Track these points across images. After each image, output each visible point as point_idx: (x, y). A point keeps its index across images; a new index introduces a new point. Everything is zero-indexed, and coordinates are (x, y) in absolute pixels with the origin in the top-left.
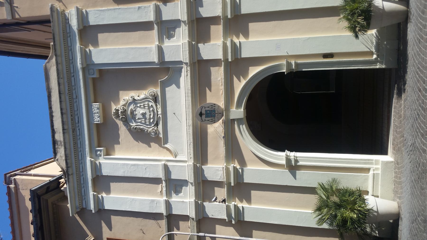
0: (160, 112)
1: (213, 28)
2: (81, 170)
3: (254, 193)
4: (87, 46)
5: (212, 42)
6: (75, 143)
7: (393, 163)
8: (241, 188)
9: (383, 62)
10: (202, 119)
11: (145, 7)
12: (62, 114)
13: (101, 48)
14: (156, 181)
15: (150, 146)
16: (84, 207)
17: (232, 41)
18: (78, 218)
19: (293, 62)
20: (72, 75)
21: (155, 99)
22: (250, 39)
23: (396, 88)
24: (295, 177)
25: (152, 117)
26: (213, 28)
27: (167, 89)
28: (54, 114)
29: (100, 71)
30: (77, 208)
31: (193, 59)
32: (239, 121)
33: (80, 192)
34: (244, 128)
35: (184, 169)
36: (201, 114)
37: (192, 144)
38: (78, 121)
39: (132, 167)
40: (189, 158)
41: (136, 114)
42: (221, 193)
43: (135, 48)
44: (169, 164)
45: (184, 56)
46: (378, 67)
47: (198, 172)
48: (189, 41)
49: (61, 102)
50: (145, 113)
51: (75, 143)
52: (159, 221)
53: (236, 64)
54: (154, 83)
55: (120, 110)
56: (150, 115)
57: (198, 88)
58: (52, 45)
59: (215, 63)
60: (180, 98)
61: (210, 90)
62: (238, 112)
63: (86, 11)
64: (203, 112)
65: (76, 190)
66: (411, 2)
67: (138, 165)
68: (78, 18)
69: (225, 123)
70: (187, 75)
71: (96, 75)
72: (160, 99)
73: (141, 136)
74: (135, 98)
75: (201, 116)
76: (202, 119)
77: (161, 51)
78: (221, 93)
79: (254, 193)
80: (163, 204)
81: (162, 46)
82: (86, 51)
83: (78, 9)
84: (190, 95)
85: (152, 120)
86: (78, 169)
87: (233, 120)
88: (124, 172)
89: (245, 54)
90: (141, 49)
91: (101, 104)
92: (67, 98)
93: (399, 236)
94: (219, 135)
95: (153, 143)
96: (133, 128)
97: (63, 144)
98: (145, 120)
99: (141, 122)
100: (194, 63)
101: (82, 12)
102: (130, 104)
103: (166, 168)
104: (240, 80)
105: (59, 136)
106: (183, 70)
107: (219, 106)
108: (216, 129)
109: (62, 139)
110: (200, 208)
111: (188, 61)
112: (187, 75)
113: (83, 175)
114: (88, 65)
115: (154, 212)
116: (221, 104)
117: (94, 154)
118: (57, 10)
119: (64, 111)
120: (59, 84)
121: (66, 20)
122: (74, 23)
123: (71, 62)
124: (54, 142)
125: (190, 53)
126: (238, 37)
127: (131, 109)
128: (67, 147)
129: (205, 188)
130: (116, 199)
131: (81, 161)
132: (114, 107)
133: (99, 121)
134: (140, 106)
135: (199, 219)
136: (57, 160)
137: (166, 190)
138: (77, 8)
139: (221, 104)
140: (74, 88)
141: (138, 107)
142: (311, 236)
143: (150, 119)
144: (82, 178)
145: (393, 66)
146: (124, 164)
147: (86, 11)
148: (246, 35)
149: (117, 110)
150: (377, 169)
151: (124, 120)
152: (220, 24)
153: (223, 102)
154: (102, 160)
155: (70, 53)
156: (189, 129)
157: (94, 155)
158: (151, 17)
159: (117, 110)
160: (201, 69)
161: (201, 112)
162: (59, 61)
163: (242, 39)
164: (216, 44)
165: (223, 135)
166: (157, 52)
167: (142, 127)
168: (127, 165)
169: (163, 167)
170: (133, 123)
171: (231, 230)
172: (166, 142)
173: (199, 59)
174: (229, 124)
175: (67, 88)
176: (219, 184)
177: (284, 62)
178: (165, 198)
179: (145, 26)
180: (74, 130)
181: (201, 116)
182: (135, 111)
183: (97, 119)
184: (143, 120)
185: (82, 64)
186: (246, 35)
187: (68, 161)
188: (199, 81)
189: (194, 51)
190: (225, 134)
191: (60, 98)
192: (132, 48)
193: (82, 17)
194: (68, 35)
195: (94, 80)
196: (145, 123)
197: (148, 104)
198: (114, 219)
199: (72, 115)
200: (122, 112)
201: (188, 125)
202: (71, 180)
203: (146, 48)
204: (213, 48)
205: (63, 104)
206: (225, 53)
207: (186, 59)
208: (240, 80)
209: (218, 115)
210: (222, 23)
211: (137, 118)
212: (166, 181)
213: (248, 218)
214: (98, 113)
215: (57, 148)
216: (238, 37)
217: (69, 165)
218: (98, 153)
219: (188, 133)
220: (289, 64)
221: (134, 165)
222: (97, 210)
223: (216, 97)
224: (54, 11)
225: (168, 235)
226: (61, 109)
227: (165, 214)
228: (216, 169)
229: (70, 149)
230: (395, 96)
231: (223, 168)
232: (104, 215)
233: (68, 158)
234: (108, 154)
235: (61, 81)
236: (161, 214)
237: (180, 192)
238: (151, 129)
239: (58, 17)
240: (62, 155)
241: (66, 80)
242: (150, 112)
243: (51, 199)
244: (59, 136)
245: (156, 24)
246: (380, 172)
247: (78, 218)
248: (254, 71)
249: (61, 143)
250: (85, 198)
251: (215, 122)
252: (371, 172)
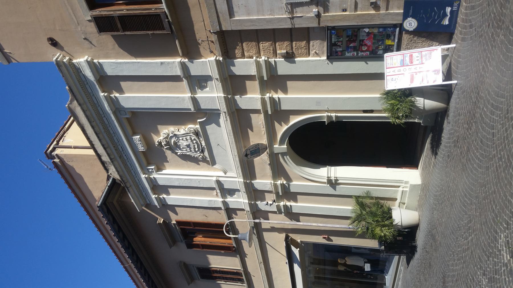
0: (203, 144)
15: (199, 164)
21: (197, 134)
25: (196, 147)
26: (248, 83)
28: (93, 143)
32: (283, 154)
34: (287, 158)
37: (240, 167)
44: (220, 179)
50: (189, 145)
53: (276, 114)
61: (252, 131)
64: (248, 152)
70: (227, 120)
78: (263, 133)
84: (232, 134)
92: (105, 135)
104: (281, 125)
112: (227, 120)
116: (264, 141)
119: (106, 146)
122: (88, 73)
124: (103, 163)
146: (178, 179)
154: (155, 175)
157: (147, 172)
160: (241, 120)
175: (101, 128)
180: (120, 157)
185: (111, 110)
191: (98, 137)
196: (191, 151)
204: (252, 98)
208: (281, 125)
221: (188, 179)
222: (161, 205)
224: (61, 66)
226: (103, 145)
235: (94, 124)
241: (98, 122)
246: (407, 189)
248: (295, 120)
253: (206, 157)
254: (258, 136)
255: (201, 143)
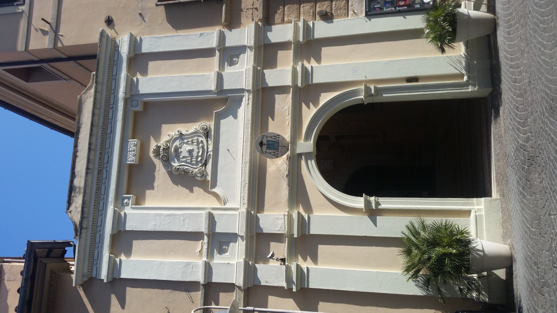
0: (211, 148)
1: (281, 54)
2: (99, 224)
3: (322, 249)
4: (134, 75)
5: (279, 68)
6: (98, 189)
7: (499, 200)
8: (305, 243)
9: (475, 84)
10: (262, 150)
11: (208, 34)
12: (90, 149)
13: (149, 76)
14: (195, 236)
16: (94, 276)
17: (303, 65)
18: (82, 293)
19: (372, 87)
20: (111, 106)
21: (207, 134)
22: (323, 64)
23: (493, 114)
24: (375, 223)
25: (200, 154)
27: (222, 121)
28: (78, 154)
29: (146, 104)
30: (83, 277)
31: (256, 85)
32: (308, 156)
33: (92, 254)
34: (313, 164)
35: (233, 222)
36: (261, 144)
37: (247, 185)
38: (108, 161)
39: (166, 219)
40: (242, 204)
41: (181, 152)
42: (280, 249)
43: (191, 76)
44: (214, 212)
45: (246, 83)
46: (470, 90)
47: (252, 222)
48: (254, 67)
49: (91, 135)
50: (193, 150)
51: (98, 189)
52: (192, 294)
53: (306, 91)
54: (208, 116)
55: (162, 146)
56: (198, 152)
57: (260, 119)
58: (94, 75)
59: (282, 90)
60: (237, 131)
62: (306, 145)
63: (141, 38)
64: (265, 141)
65: (88, 251)
66: (497, 2)
67: (174, 215)
68: (130, 44)
69: (289, 158)
70: (248, 104)
71: (140, 108)
72: (213, 134)
73: (184, 179)
74: (183, 133)
75: (261, 147)
76: (262, 150)
77: (220, 78)
78: (287, 123)
79: (322, 249)
80: (201, 268)
81: (223, 73)
82: (132, 80)
83: (131, 35)
84: (250, 125)
85: (200, 158)
86: (95, 222)
87: (300, 155)
88: (155, 225)
89: (317, 79)
90: (199, 78)
91: (139, 142)
92: (100, 131)
93: (515, 287)
94: (282, 174)
95: (197, 187)
96: (175, 168)
97: (82, 190)
98: (191, 159)
99: (185, 162)
100: (258, 91)
101: (136, 39)
102: (176, 139)
103: (212, 220)
105: (79, 182)
106: (244, 99)
107: (284, 138)
108: (277, 166)
109: (82, 185)
110: (250, 272)
111: (250, 88)
112: (248, 104)
113: (100, 231)
114: (132, 96)
115: (188, 280)
116: (287, 136)
117: (119, 201)
118: (108, 35)
119: (92, 147)
120: (93, 114)
121: (116, 48)
122: (124, 50)
123: (112, 92)
124: (72, 189)
125: (253, 78)
126: (309, 62)
127: (176, 146)
128: (87, 192)
129: (258, 242)
130: (138, 263)
131: (101, 212)
132: (153, 145)
133: (133, 161)
134: (188, 142)
135: (248, 288)
136: (70, 212)
137: (208, 249)
138: (131, 35)
139: (287, 136)
140: (110, 121)
141: (184, 143)
142: (398, 308)
143: (197, 157)
144: (98, 235)
145: (486, 92)
146: (156, 215)
147: (141, 38)
148: (318, 59)
149: (159, 147)
150: (479, 210)
151: (165, 159)
152: (290, 49)
153: (289, 134)
154: (128, 210)
155: (114, 82)
156: (245, 167)
157: (119, 205)
158: (213, 43)
159: (159, 147)
160: (264, 96)
161: (262, 142)
162: (99, 89)
163: (313, 63)
164: (284, 70)
165: (287, 173)
166: (216, 79)
167: (187, 167)
168: (161, 215)
169: (208, 215)
170: (175, 162)
171: (290, 302)
172: (214, 185)
173: (264, 86)
174: (295, 162)
175: (102, 120)
176: (277, 237)
177: (363, 87)
178: (205, 259)
179: (206, 53)
180: (100, 172)
181: (261, 147)
182: (181, 148)
183: (131, 158)
184: (189, 158)
185: (126, 93)
186: (318, 59)
187: (85, 209)
188: (261, 118)
189: (258, 77)
190: (289, 172)
191: (91, 130)
192: (188, 76)
193: (135, 44)
194: (115, 63)
195: (136, 114)
196: (191, 163)
197: (198, 140)
198: (131, 292)
199: (101, 153)
200: (164, 148)
201: (244, 162)
202: (83, 235)
203: (204, 75)
204: (282, 74)
205: (94, 138)
206: (294, 80)
207: (248, 86)
209: (281, 149)
210: (292, 48)
211: (181, 157)
212: (208, 236)
213: (314, 284)
214: (134, 151)
215: (74, 196)
216: (309, 62)
217: (85, 215)
218: (125, 201)
219: (243, 172)
220: (367, 89)
221: (170, 215)
222: (110, 279)
223: (280, 126)
224: (104, 36)
225: (204, 309)
226: (90, 144)
227: (202, 281)
228: (275, 218)
229: (91, 187)
230: (493, 118)
231: (285, 215)
232: (119, 285)
233: (85, 206)
234: (138, 202)
235: (97, 111)
236: (197, 283)
237: (225, 251)
238: (196, 170)
239: (107, 44)
240: (77, 206)
241: (102, 111)
242: (198, 149)
243: (52, 265)
244: (79, 182)
245: (218, 50)
246: (483, 213)
247: (82, 293)
248: (325, 98)
249: (80, 190)
250: (97, 264)
251: (277, 157)
252: (473, 214)
253: (207, 174)
254: (280, 126)
255: (208, 148)
